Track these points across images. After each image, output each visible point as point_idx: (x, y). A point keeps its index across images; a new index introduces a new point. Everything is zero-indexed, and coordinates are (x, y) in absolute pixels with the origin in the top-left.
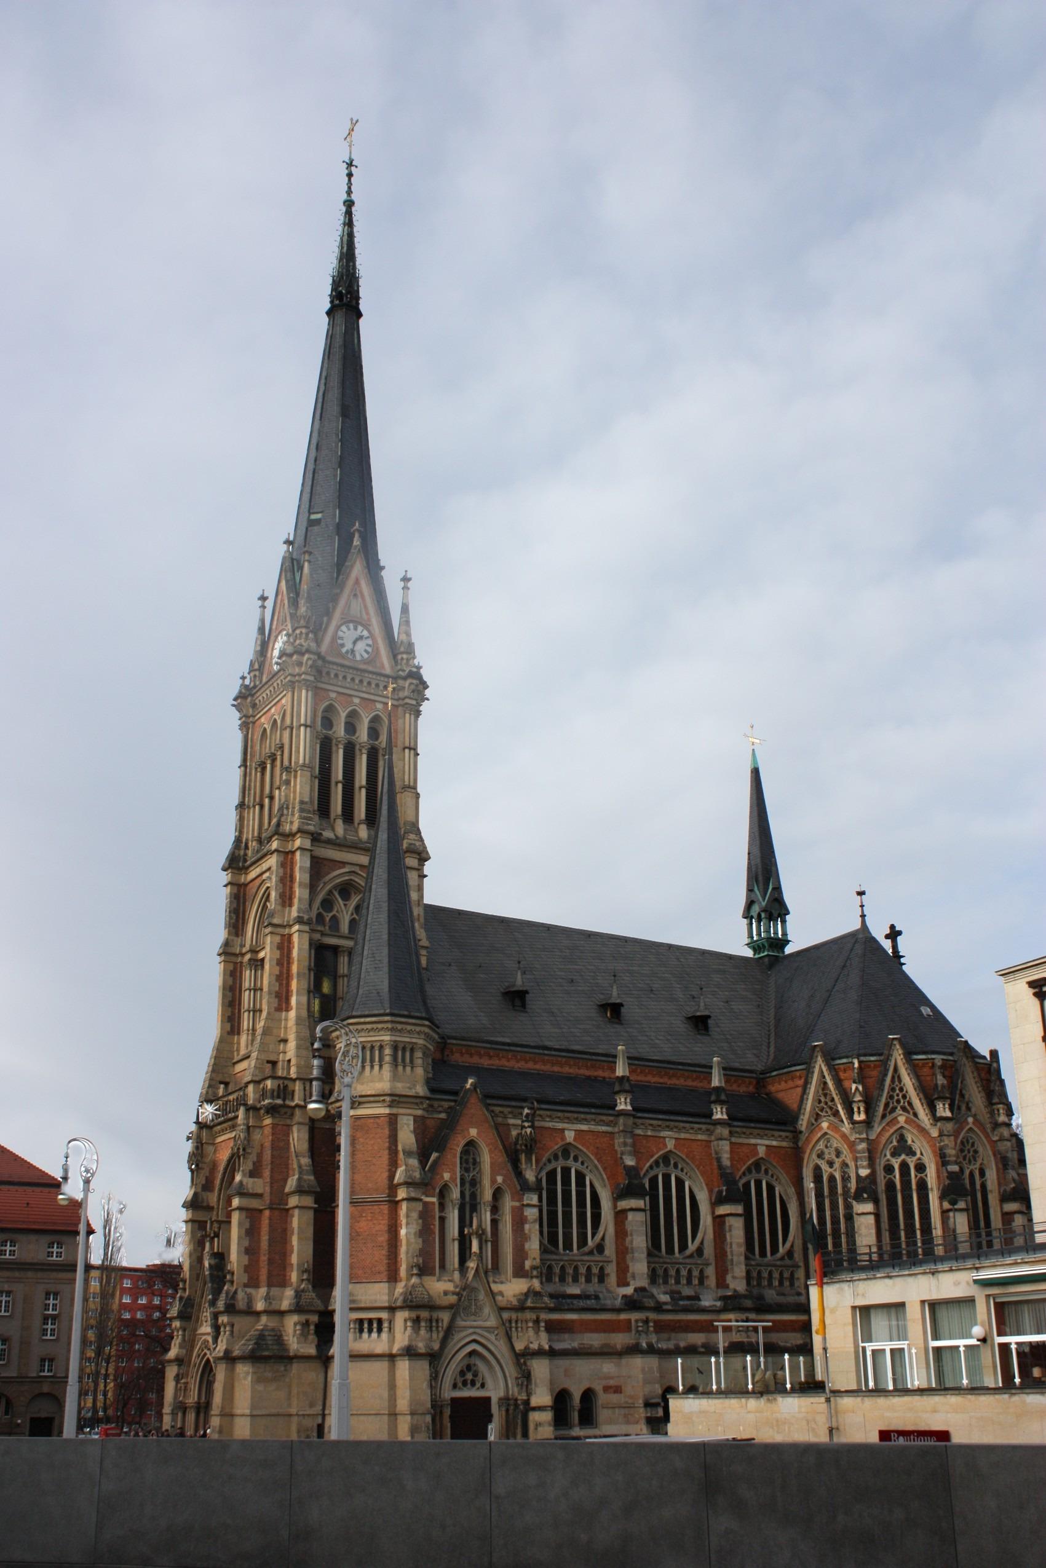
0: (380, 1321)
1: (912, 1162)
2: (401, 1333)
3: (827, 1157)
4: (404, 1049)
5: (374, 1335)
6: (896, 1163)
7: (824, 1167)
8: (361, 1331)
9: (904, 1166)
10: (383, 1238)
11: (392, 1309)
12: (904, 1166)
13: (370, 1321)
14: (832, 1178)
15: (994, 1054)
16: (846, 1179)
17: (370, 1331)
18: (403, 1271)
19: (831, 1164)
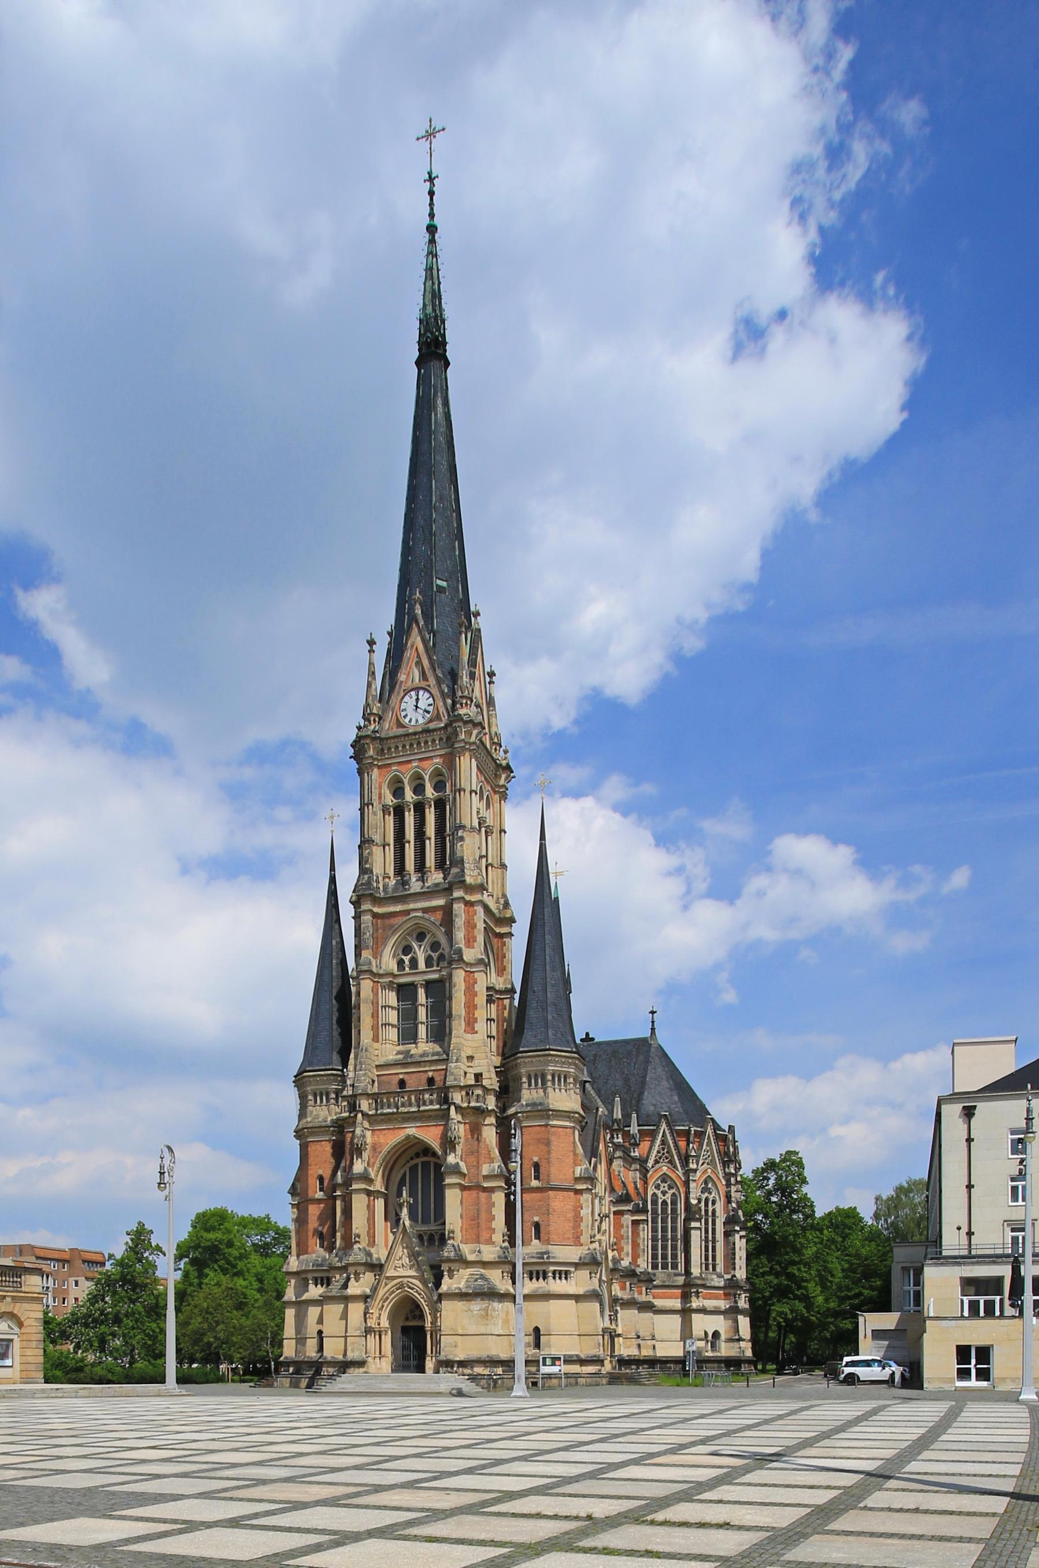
0: (567, 1273)
1: (711, 1197)
2: (580, 1282)
3: (662, 1185)
4: (536, 1076)
5: (564, 1281)
6: (704, 1196)
7: (659, 1193)
8: (554, 1278)
9: (707, 1200)
10: (570, 1215)
11: (576, 1265)
12: (707, 1200)
13: (560, 1272)
14: (664, 1202)
15: (731, 1129)
16: (674, 1203)
17: (560, 1278)
18: (585, 1238)
19: (664, 1193)
